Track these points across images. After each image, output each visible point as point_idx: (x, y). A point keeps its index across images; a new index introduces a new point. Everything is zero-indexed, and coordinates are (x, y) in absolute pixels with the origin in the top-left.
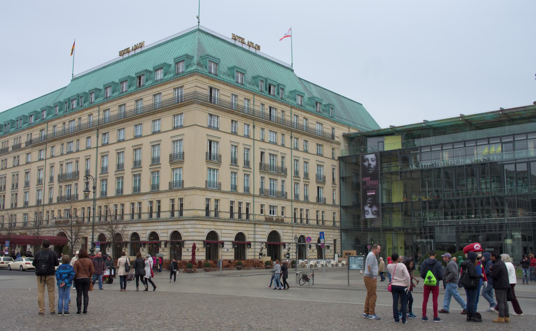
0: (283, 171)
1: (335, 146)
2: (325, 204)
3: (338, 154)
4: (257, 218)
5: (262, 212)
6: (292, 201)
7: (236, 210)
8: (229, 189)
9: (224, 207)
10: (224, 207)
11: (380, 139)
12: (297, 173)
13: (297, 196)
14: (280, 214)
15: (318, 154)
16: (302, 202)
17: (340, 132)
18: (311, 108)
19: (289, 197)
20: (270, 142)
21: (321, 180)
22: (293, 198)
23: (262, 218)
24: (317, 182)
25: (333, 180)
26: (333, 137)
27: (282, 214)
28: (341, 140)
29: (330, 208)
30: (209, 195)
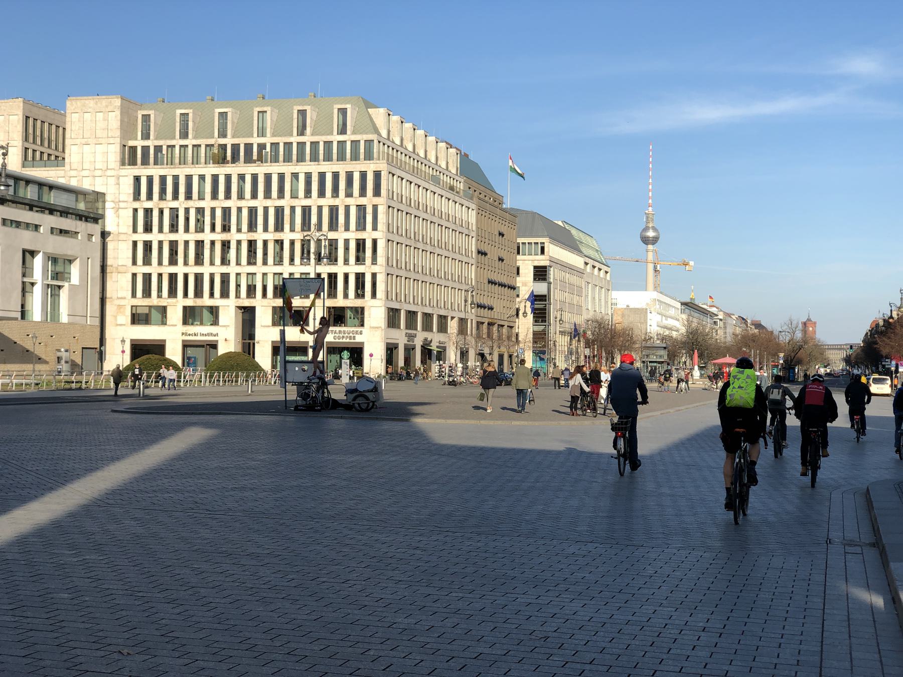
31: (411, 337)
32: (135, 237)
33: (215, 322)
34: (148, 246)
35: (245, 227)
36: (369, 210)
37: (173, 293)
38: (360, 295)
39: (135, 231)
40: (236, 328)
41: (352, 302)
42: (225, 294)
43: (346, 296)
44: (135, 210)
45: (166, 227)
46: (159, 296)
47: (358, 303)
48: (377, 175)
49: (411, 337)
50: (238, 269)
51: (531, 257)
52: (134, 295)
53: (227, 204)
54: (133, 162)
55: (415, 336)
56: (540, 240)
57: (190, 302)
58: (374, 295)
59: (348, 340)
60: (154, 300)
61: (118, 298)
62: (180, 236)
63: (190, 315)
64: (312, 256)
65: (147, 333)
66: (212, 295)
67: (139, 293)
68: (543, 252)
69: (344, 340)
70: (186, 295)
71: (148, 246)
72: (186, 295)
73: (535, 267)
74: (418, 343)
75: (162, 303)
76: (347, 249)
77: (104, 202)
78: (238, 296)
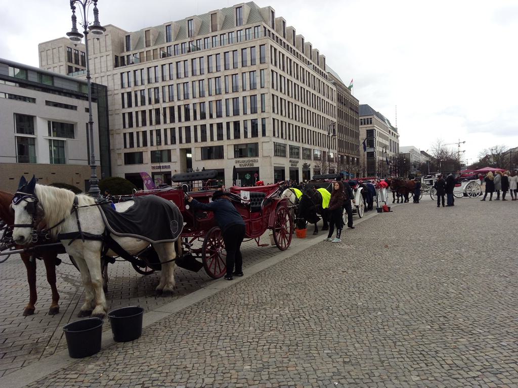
32: (124, 111)
33: (170, 160)
37: (145, 144)
38: (255, 134)
40: (181, 162)
41: (250, 140)
42: (173, 142)
43: (246, 136)
45: (139, 103)
47: (254, 140)
50: (180, 125)
51: (365, 126)
55: (298, 162)
56: (371, 117)
57: (154, 148)
59: (249, 167)
60: (136, 149)
61: (118, 149)
62: (191, 123)
66: (166, 144)
67: (128, 146)
68: (371, 123)
69: (247, 167)
70: (152, 145)
72: (152, 145)
73: (367, 130)
75: (140, 150)
77: (106, 91)
78: (181, 142)
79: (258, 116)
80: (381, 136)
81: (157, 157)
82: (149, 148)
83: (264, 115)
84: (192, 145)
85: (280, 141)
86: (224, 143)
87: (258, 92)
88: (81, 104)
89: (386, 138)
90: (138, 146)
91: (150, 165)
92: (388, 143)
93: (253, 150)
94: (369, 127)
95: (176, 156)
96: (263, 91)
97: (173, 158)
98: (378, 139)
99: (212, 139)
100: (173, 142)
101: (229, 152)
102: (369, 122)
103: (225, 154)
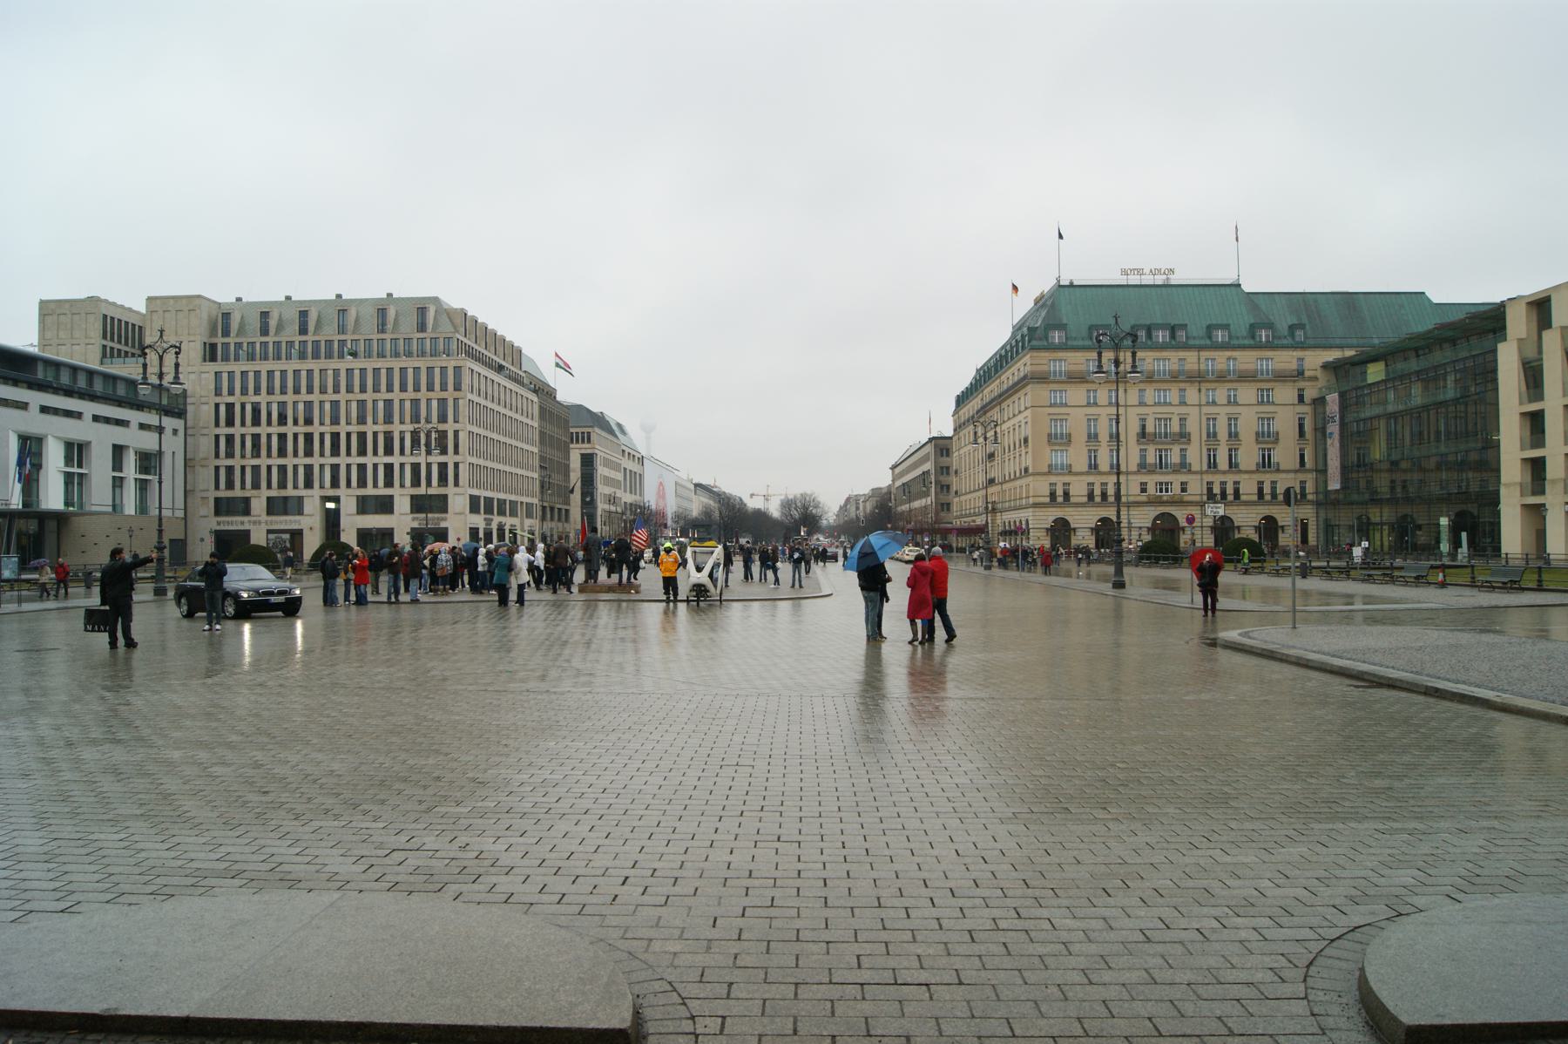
0: (1184, 436)
1: (1302, 384)
2: (1278, 470)
3: (1310, 394)
4: (1131, 499)
5: (1144, 490)
6: (1201, 473)
7: (1097, 492)
8: (1085, 468)
9: (1079, 490)
10: (1079, 490)
11: (1358, 369)
12: (1212, 436)
13: (1212, 465)
14: (1176, 489)
15: (1262, 403)
16: (1224, 472)
17: (1315, 360)
18: (1246, 342)
19: (1196, 467)
20: (1158, 404)
21: (1267, 438)
22: (1205, 467)
23: (1143, 498)
24: (1258, 442)
25: (1302, 433)
26: (1300, 373)
27: (1184, 490)
28: (1319, 373)
29: (1292, 475)
30: (1053, 479)
31: (489, 522)
34: (230, 439)
35: (327, 420)
36: (450, 403)
39: (217, 424)
41: (435, 490)
42: (309, 484)
44: (217, 406)
46: (243, 487)
47: (442, 491)
48: (457, 369)
49: (489, 522)
52: (217, 487)
53: (309, 398)
54: (213, 359)
57: (274, 493)
58: (456, 484)
60: (237, 492)
63: (274, 507)
64: (423, 448)
65: (234, 523)
71: (230, 439)
72: (269, 486)
74: (494, 527)
75: (247, 494)
76: (402, 440)
79: (450, 459)
80: (608, 463)
81: (277, 506)
82: (265, 493)
83: (458, 458)
84: (342, 492)
85: (476, 492)
86: (395, 491)
87: (450, 427)
88: (169, 423)
89: (616, 467)
90: (243, 487)
91: (264, 517)
92: (619, 476)
93: (440, 503)
94: (586, 448)
95: (312, 505)
96: (457, 426)
97: (307, 508)
98: (601, 471)
99: (375, 485)
100: (309, 484)
101: (402, 504)
102: (587, 438)
103: (396, 507)
